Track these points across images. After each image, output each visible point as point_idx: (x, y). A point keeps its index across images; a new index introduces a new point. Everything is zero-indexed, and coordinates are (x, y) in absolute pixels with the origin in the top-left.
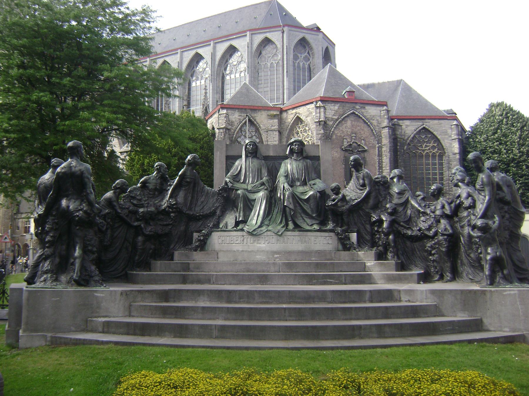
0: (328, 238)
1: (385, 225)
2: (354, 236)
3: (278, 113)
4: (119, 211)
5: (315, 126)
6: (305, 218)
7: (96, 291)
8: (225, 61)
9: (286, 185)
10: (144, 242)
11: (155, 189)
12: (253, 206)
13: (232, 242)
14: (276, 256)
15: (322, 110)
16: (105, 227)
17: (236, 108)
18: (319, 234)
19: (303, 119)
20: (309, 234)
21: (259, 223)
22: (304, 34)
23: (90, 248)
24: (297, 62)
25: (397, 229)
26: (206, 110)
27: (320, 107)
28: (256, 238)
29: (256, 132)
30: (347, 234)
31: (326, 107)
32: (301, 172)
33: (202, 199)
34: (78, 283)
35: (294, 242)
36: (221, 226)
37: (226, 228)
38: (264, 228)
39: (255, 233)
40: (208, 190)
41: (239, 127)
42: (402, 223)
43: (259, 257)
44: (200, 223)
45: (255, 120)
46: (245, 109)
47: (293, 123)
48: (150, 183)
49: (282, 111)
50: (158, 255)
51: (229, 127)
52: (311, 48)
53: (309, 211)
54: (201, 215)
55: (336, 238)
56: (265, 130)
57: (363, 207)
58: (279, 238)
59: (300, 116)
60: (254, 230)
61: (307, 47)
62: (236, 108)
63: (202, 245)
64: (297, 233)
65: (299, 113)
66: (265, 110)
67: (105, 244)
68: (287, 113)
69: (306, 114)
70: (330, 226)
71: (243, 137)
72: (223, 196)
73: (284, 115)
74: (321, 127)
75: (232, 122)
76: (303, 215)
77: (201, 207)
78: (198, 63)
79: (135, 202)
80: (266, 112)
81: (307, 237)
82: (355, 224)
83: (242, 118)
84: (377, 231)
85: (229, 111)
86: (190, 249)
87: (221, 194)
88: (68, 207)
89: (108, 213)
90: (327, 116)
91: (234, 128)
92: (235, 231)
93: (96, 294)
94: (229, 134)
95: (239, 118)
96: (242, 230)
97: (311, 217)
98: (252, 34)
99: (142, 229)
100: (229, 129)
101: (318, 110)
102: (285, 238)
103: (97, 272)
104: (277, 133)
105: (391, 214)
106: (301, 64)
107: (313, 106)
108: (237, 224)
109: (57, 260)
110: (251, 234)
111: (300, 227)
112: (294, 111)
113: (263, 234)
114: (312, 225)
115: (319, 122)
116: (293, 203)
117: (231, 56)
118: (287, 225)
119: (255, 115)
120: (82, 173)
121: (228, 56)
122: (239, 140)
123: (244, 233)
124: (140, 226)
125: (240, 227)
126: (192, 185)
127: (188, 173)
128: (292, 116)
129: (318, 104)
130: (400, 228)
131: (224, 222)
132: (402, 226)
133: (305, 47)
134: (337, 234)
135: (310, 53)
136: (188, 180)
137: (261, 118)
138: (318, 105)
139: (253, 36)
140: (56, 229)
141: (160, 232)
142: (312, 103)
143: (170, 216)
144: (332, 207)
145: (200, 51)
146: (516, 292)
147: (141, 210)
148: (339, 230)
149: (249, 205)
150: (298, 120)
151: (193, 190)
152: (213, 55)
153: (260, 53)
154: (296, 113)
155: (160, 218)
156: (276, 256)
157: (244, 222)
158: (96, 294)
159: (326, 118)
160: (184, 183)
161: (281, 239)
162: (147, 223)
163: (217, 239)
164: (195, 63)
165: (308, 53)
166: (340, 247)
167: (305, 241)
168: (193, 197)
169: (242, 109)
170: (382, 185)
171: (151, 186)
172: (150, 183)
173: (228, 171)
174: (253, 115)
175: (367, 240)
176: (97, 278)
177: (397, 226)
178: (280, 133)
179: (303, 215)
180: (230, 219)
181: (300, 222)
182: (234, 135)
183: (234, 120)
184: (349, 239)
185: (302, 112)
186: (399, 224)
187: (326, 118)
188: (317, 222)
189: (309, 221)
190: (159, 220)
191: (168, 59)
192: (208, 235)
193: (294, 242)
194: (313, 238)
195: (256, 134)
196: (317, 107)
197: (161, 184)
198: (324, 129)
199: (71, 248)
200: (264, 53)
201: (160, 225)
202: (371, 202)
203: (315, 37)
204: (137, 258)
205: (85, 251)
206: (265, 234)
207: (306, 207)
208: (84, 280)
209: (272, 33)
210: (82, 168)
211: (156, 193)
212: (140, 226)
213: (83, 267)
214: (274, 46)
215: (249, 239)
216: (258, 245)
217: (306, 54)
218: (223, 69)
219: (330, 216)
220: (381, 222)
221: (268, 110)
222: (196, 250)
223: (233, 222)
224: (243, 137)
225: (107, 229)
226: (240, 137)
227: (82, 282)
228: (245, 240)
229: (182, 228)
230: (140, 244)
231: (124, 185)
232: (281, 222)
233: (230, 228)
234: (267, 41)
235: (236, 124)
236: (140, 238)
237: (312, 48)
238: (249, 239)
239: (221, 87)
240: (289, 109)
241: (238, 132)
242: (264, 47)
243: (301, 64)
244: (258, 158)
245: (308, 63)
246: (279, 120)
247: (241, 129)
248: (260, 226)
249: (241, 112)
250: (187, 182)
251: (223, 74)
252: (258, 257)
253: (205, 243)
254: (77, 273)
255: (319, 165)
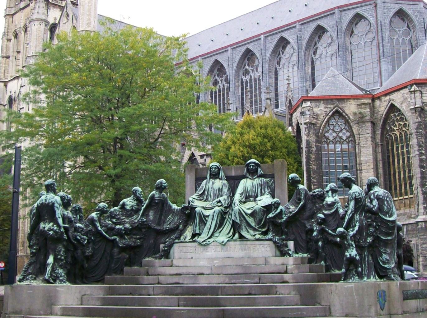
0: (265, 246)
1: (315, 233)
2: (291, 244)
3: (370, 101)
4: (99, 228)
5: (410, 114)
6: (249, 230)
7: (58, 287)
8: (313, 44)
9: (237, 203)
10: (119, 253)
11: (132, 210)
12: (207, 221)
13: (187, 252)
14: (215, 262)
15: (418, 94)
16: (86, 242)
17: (321, 100)
18: (257, 242)
19: (398, 106)
20: (249, 243)
21: (209, 236)
22: (401, 5)
23: (59, 257)
24: (395, 38)
25: (326, 237)
26: (290, 102)
27: (414, 91)
28: (206, 247)
29: (345, 124)
30: (285, 242)
31: (422, 90)
32: (254, 190)
33: (170, 217)
34: (48, 281)
35: (237, 250)
36: (182, 238)
37: (185, 240)
38: (211, 240)
39: (205, 243)
40: (174, 209)
41: (326, 120)
42: (330, 231)
43: (202, 263)
44: (166, 237)
45: (344, 111)
46: (332, 100)
47: (387, 112)
48: (127, 205)
49: (374, 99)
50: (130, 263)
51: (314, 121)
52: (411, 21)
53: (253, 224)
54: (166, 230)
55: (273, 246)
56: (356, 122)
57: (300, 219)
58: (223, 247)
59: (394, 103)
60: (204, 241)
61: (405, 19)
62: (321, 100)
63: (166, 255)
64: (238, 243)
65: (393, 100)
66: (354, 99)
67: (87, 254)
68: (380, 100)
69: (400, 100)
70: (270, 236)
71: (331, 131)
72: (185, 213)
73: (377, 103)
74: (418, 113)
75: (317, 115)
76: (247, 228)
77: (169, 223)
78: (284, 48)
79: (114, 220)
80: (356, 101)
81: (247, 246)
82: (293, 233)
83: (328, 110)
84: (310, 239)
85: (313, 104)
86: (156, 258)
87: (183, 212)
88: (44, 228)
89: (90, 231)
90: (425, 101)
91: (319, 122)
92: (190, 242)
93: (58, 289)
94: (315, 130)
95: (325, 110)
96: (195, 241)
97: (255, 230)
98: (341, 11)
99: (117, 242)
100: (314, 124)
101: (413, 96)
102: (228, 247)
103: (63, 274)
104: (369, 124)
105: (319, 224)
106: (400, 40)
107: (406, 91)
108: (194, 235)
109: (38, 266)
110: (200, 244)
111: (245, 238)
112: (387, 98)
113: (211, 245)
114: (254, 235)
115: (415, 109)
116: (240, 217)
117: (320, 37)
118: (234, 235)
119: (344, 105)
120: (53, 204)
121: (317, 39)
122: (327, 135)
123: (196, 244)
124: (115, 240)
125: (196, 238)
126: (160, 206)
127: (157, 196)
128: (386, 103)
129: (413, 88)
130: (329, 237)
131: (185, 234)
132: (330, 234)
133: (403, 20)
134: (275, 242)
135: (410, 26)
136: (157, 201)
137: (350, 108)
138: (412, 89)
139: (343, 13)
140: (38, 244)
141: (133, 244)
142: (406, 87)
143: (142, 231)
144: (272, 220)
145: (285, 35)
146: (353, 285)
147: (118, 227)
148: (277, 238)
149: (203, 220)
150: (392, 108)
151: (162, 210)
152: (299, 39)
153: (352, 32)
154: (390, 101)
155: (134, 233)
156: (215, 262)
157: (199, 235)
158: (58, 289)
159: (423, 103)
160: (153, 204)
161: (225, 248)
162: (121, 236)
163: (176, 250)
164: (281, 49)
165: (408, 27)
166: (278, 253)
167: (245, 250)
168: (161, 215)
169: (327, 100)
170: (318, 198)
171: (128, 208)
172: (127, 205)
173: (196, 190)
174: (340, 106)
175: (302, 247)
176: (61, 278)
177: (325, 234)
178: (373, 124)
179: (247, 228)
180: (188, 234)
181: (244, 233)
182: (320, 129)
183: (319, 113)
184: (286, 246)
185: (397, 98)
186: (327, 232)
187: (423, 103)
188: (260, 233)
189: (252, 232)
190: (134, 235)
191: (250, 47)
192: (170, 246)
193: (236, 250)
194: (252, 247)
195: (346, 127)
196: (411, 92)
197: (138, 205)
198: (420, 116)
199: (47, 258)
200: (355, 31)
201: (134, 238)
202: (307, 213)
203: (414, 7)
204: (113, 265)
205: (55, 259)
206: (212, 244)
207: (251, 220)
208: (53, 279)
209: (363, 8)
210: (53, 200)
211: (133, 213)
212: (115, 240)
213: (53, 270)
214: (367, 21)
215: (199, 249)
216: (207, 253)
217: (405, 27)
218: (312, 52)
219: (271, 228)
220: (312, 231)
221: (357, 99)
222: (161, 259)
223: (191, 234)
224: (331, 131)
225: (88, 242)
226: (327, 132)
227: (52, 281)
228: (197, 250)
229: (152, 241)
230: (116, 254)
231: (104, 208)
232: (229, 233)
233: (187, 240)
234: (358, 18)
235: (322, 117)
236: (116, 250)
237: (412, 20)
238: (200, 248)
239: (310, 74)
240: (382, 96)
241: (325, 125)
242: (356, 24)
243: (400, 40)
244: (221, 179)
245: (408, 38)
246: (371, 109)
247: (328, 122)
248: (208, 238)
249: (327, 104)
250: (156, 202)
251: (312, 59)
252: (201, 263)
253: (169, 252)
254: (48, 275)
255: (274, 182)
